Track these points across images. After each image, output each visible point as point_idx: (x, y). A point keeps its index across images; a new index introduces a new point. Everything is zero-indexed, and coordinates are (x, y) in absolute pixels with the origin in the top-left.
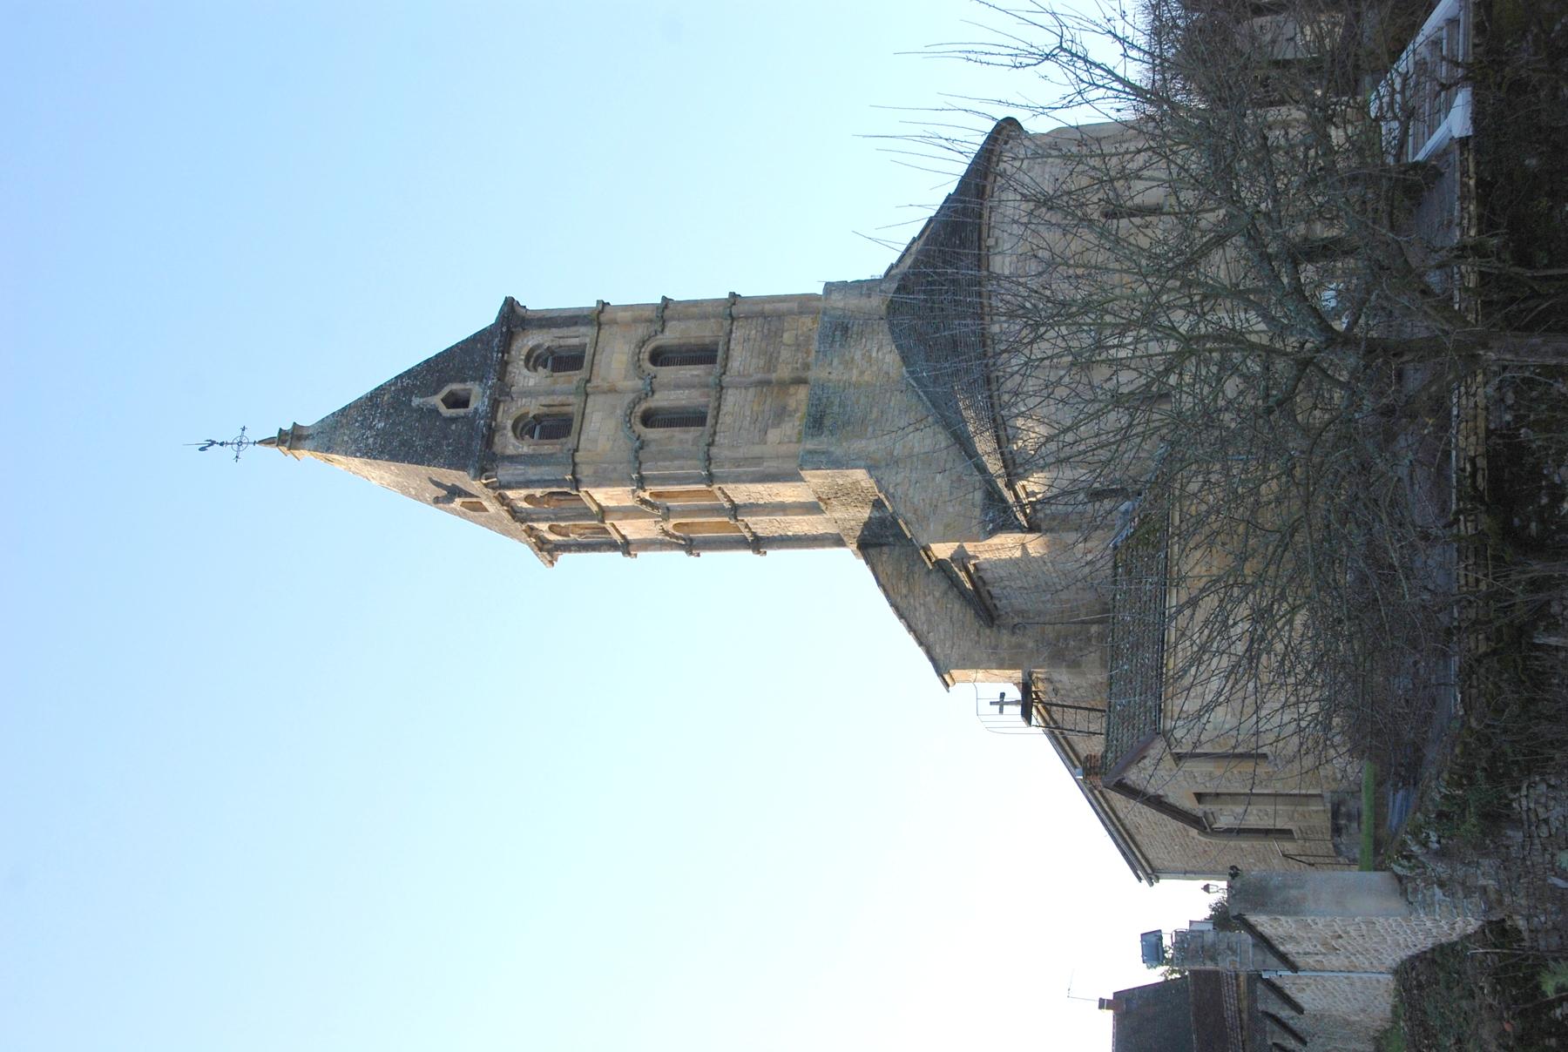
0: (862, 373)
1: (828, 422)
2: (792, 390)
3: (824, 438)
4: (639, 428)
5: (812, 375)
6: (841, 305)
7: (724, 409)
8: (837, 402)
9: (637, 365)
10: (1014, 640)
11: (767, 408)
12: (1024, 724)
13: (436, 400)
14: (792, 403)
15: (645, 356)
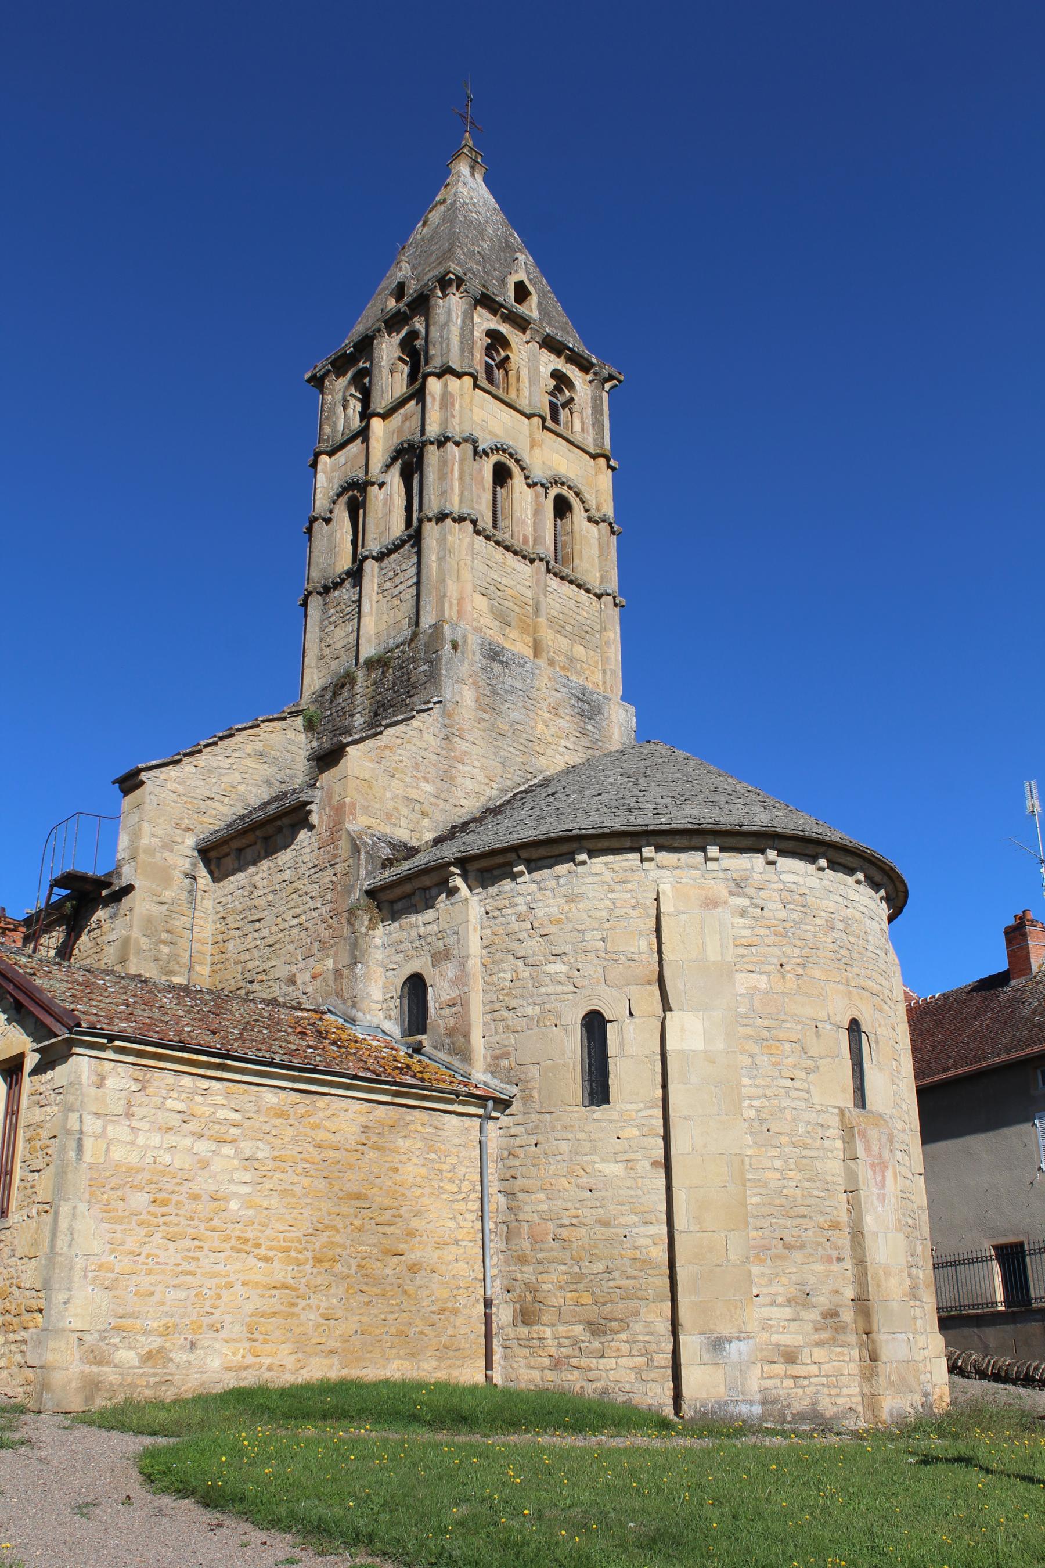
0: (545, 723)
1: (495, 665)
2: (529, 639)
3: (478, 657)
4: (494, 458)
5: (542, 662)
6: (614, 718)
7: (510, 555)
8: (518, 685)
9: (557, 481)
10: (178, 875)
11: (510, 604)
12: (57, 874)
13: (521, 276)
14: (514, 634)
15: (564, 491)
